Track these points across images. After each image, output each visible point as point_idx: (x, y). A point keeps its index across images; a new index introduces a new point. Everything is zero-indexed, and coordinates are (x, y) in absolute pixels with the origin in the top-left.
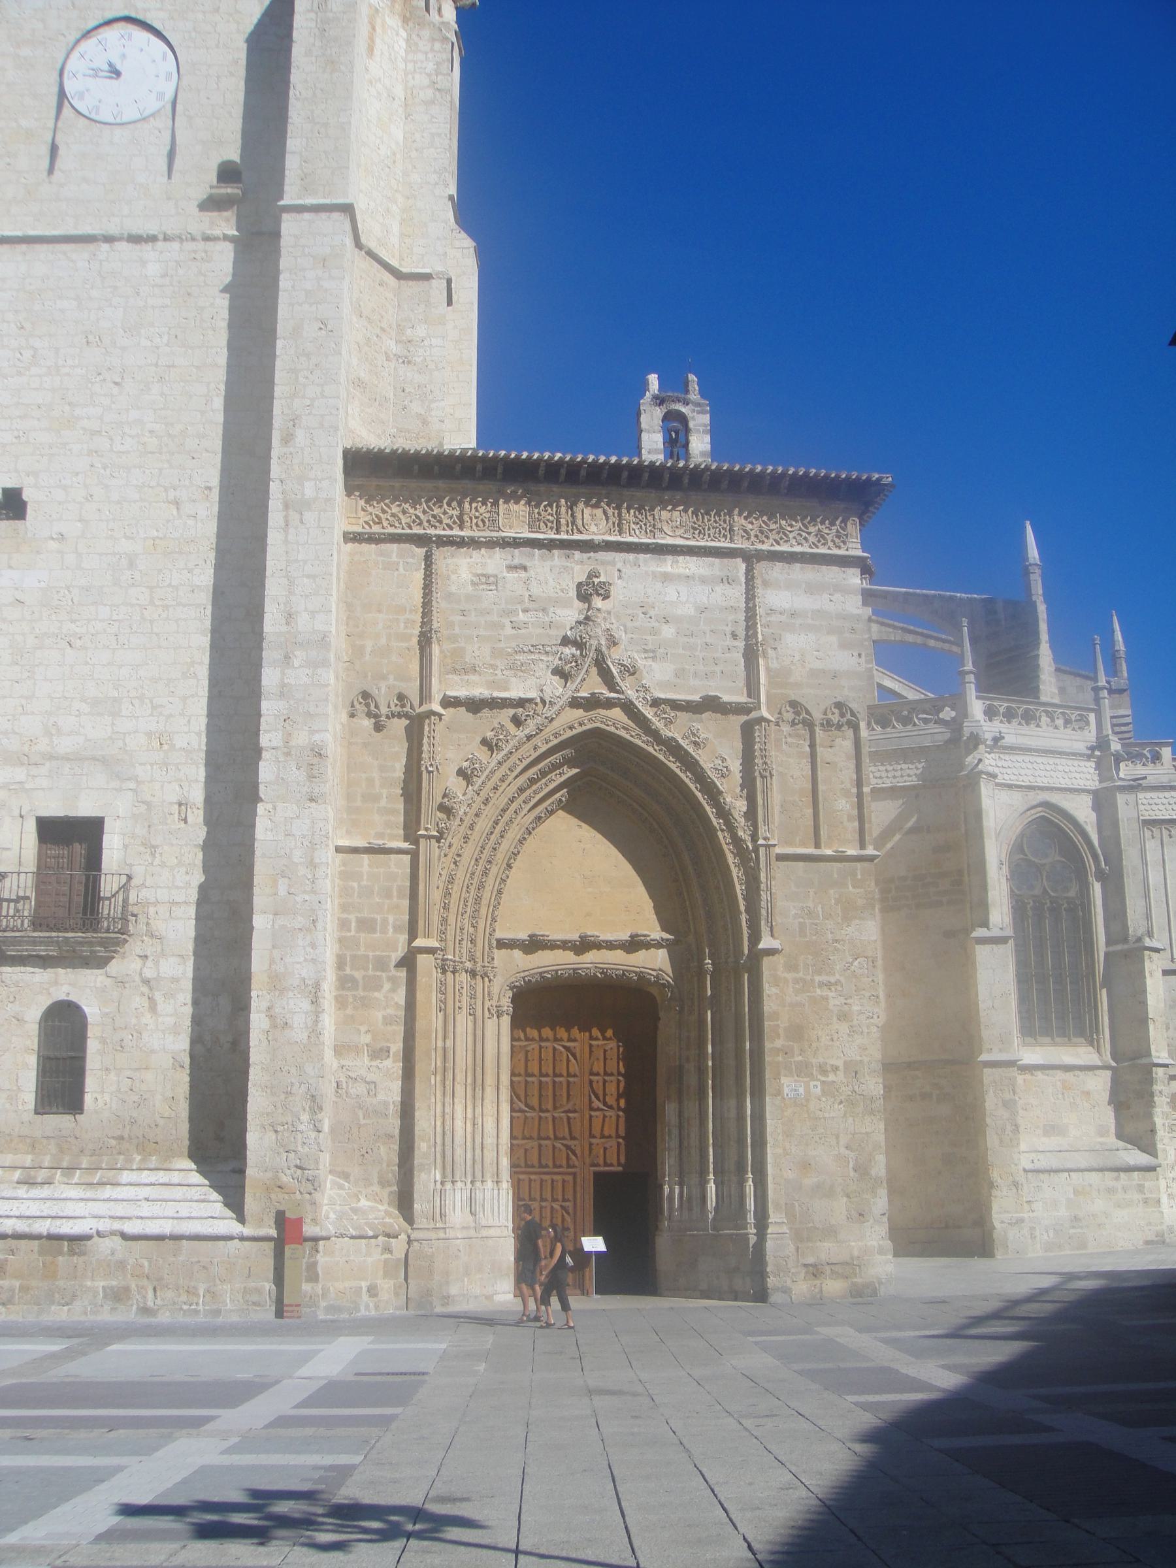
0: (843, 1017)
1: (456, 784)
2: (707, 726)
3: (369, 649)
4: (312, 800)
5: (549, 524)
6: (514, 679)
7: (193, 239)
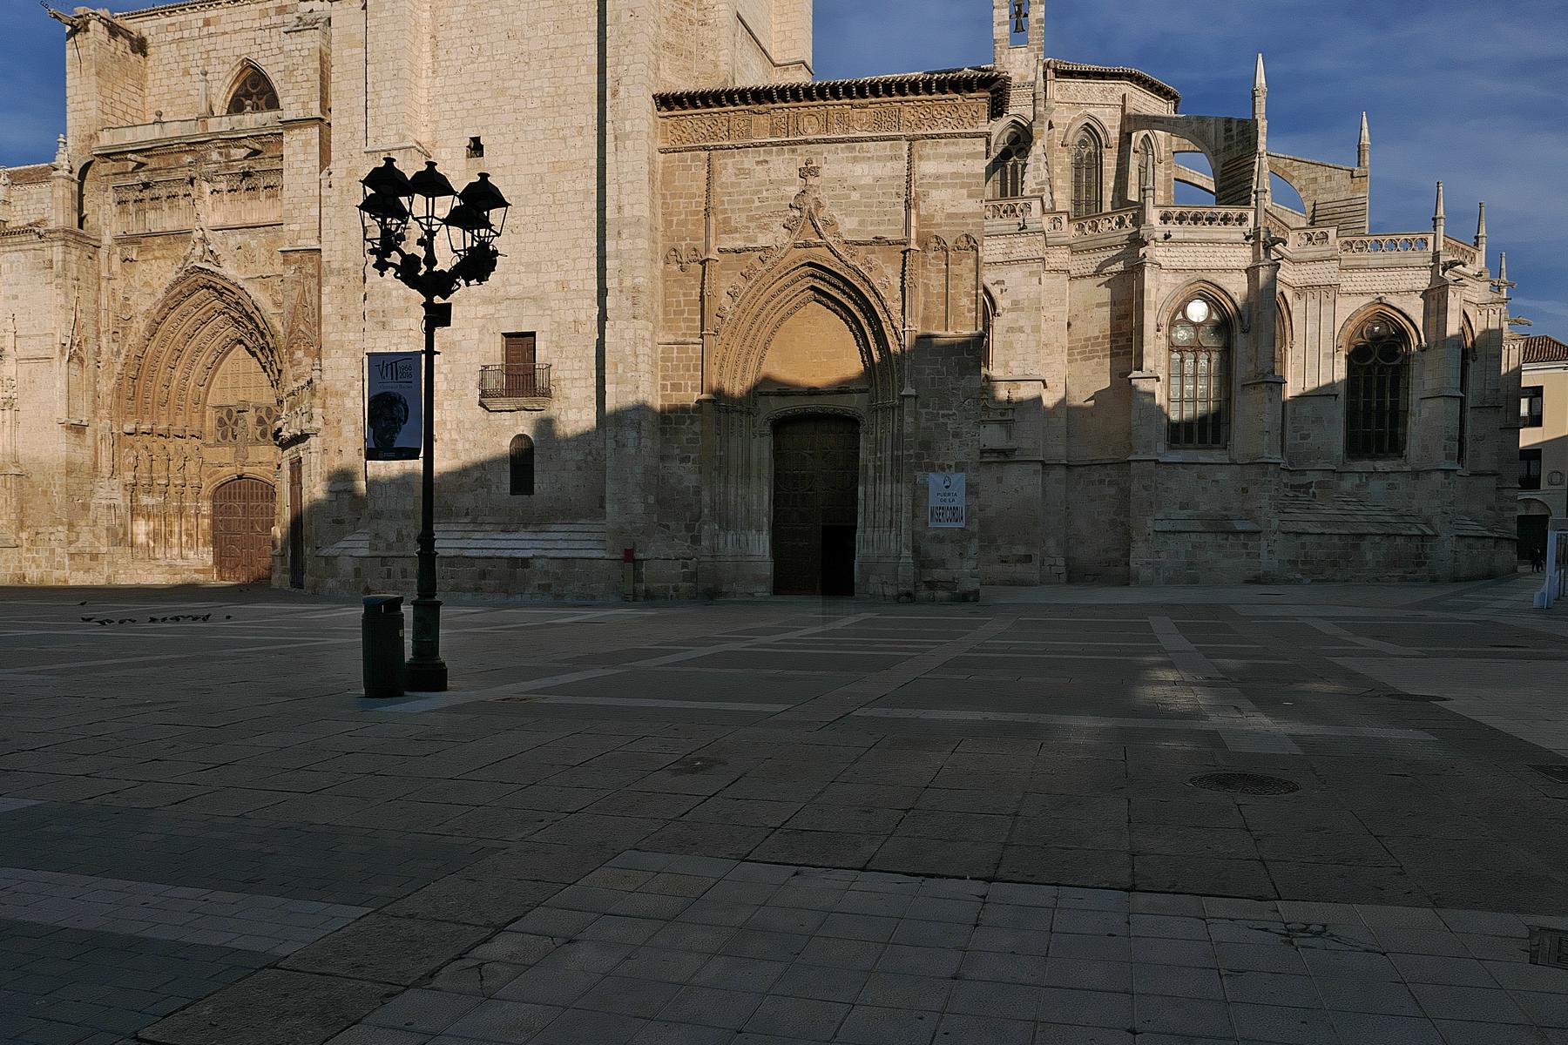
0: (956, 435)
1: (725, 300)
2: (877, 259)
3: (675, 222)
4: (634, 318)
5: (783, 130)
6: (760, 235)
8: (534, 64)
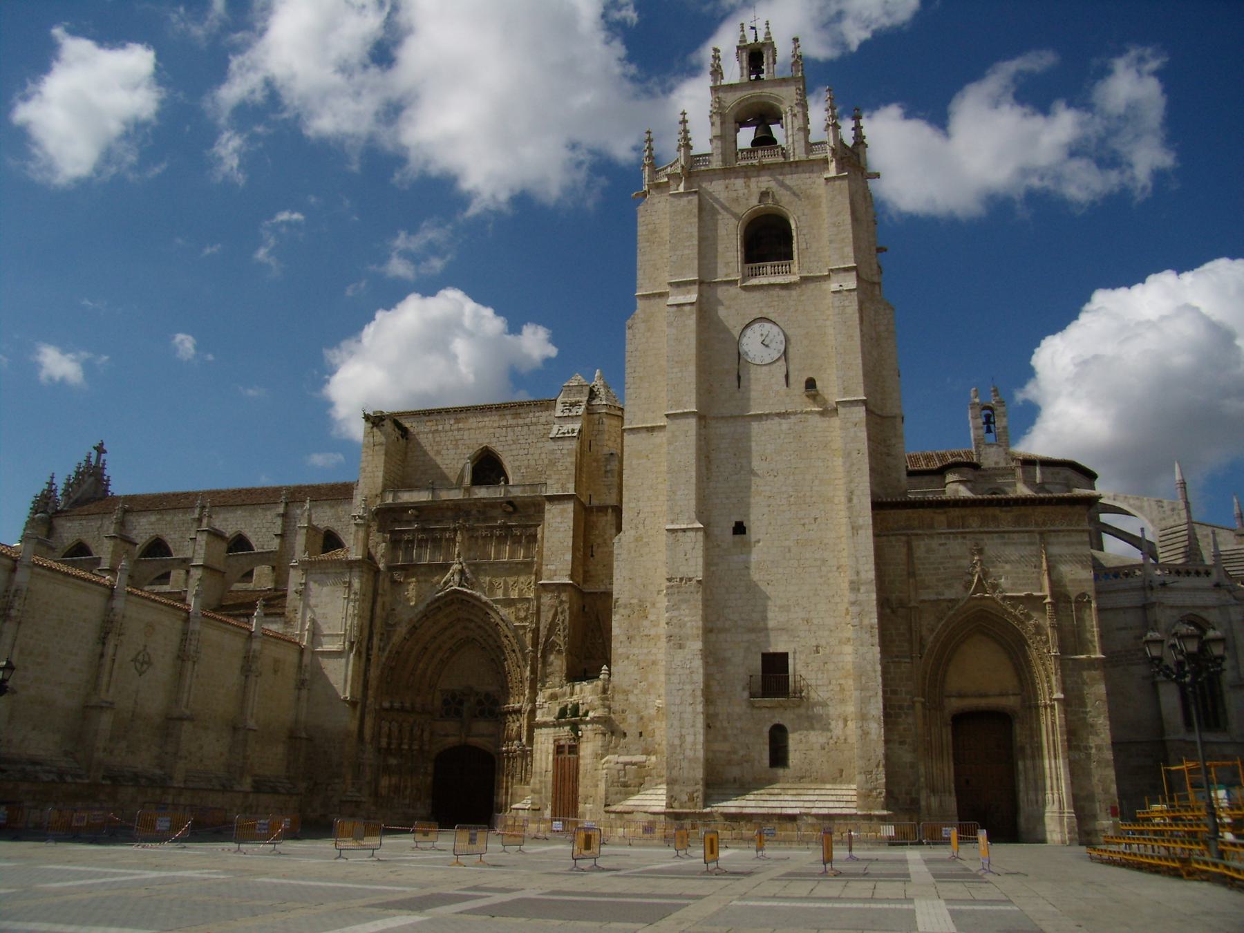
4: (872, 645)
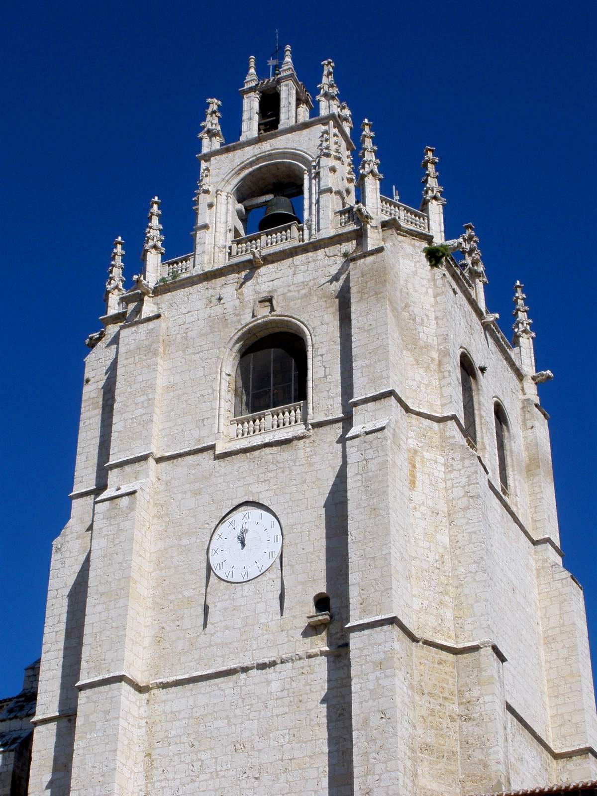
7: (300, 659)
8: (266, 779)
